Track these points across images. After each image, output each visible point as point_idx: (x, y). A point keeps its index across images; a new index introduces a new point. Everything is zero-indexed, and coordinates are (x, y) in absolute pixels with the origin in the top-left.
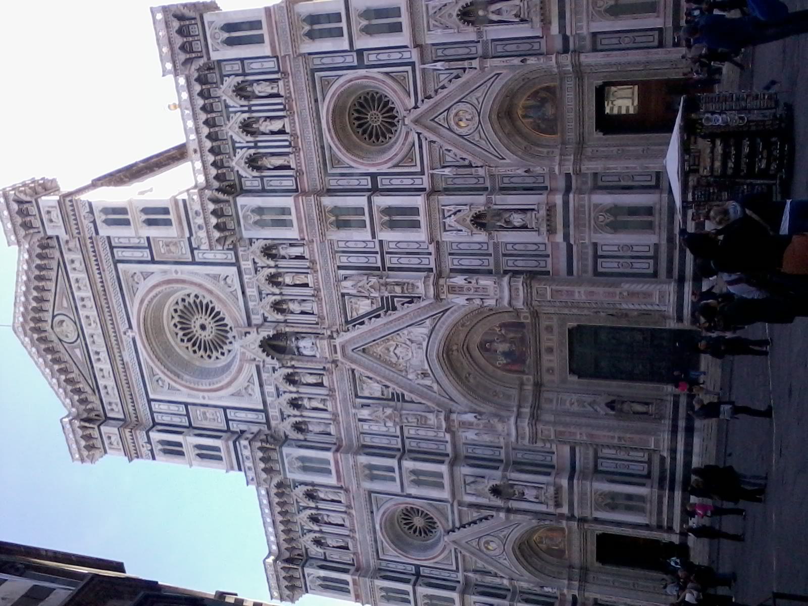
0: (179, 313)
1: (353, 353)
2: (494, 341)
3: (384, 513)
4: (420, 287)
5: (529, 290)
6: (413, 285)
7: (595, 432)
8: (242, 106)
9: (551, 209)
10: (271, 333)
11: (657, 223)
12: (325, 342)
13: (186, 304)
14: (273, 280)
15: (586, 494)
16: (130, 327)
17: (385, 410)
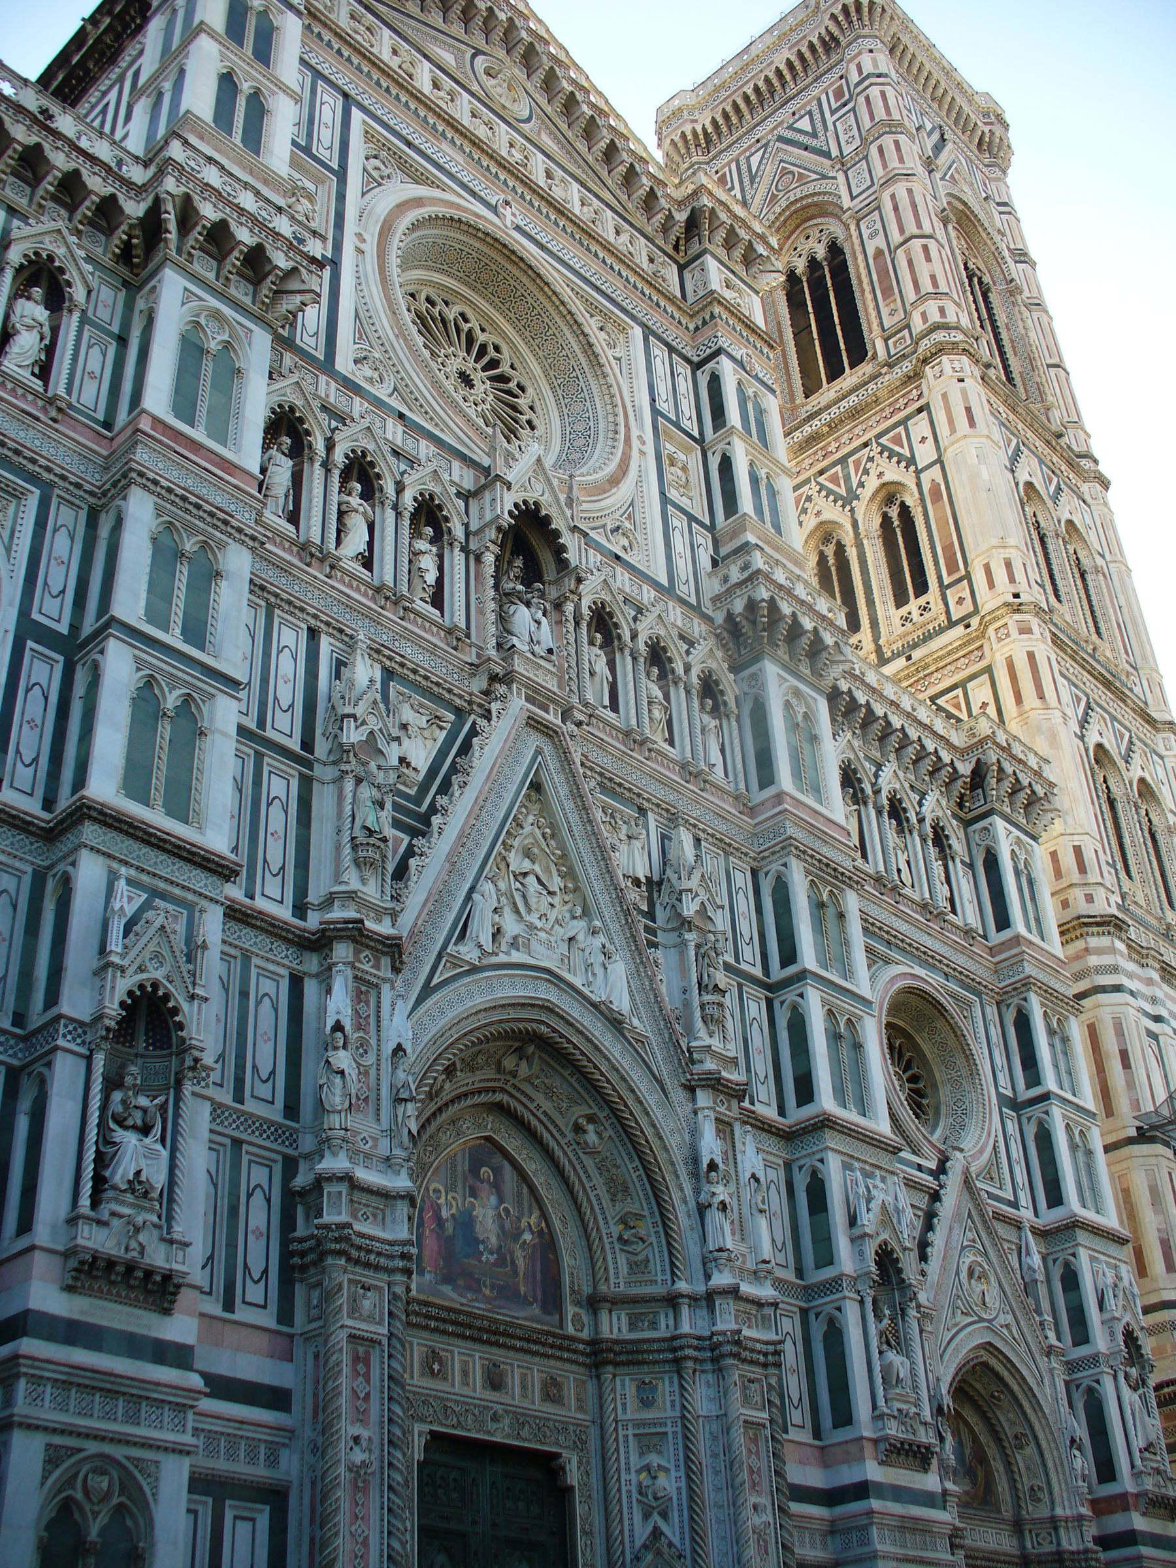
0: (492, 353)
2: (501, 1200)
5: (762, 1358)
13: (512, 385)
14: (657, 656)
16: (518, 228)
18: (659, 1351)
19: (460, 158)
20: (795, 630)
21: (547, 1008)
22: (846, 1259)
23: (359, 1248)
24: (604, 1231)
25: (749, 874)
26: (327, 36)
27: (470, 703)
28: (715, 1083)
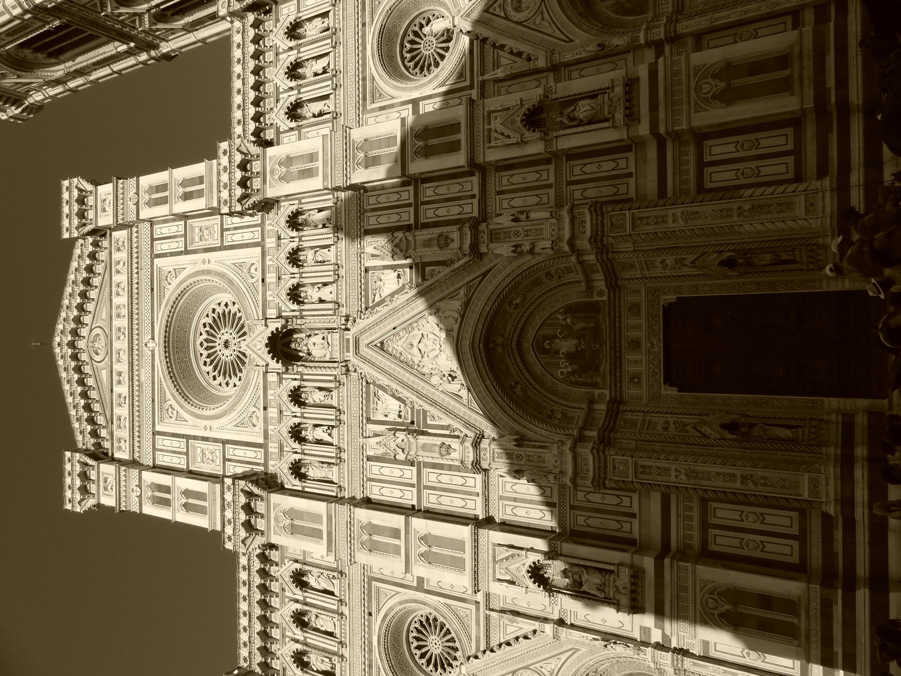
1: (366, 350)
2: (556, 337)
3: (386, 616)
4: (455, 239)
5: (600, 218)
6: (447, 237)
7: (701, 467)
8: (291, 49)
9: (631, 84)
10: (279, 326)
11: (796, 76)
12: (336, 336)
13: (215, 316)
14: (294, 258)
15: (685, 589)
16: (153, 338)
17: (397, 435)
18: (606, 264)
19: (143, 371)
20: (243, 183)
21: (472, 346)
22: (536, 148)
23: (600, 473)
24: (557, 284)
25: (369, 194)
26: (137, 444)
27: (362, 378)
28: (474, 247)
